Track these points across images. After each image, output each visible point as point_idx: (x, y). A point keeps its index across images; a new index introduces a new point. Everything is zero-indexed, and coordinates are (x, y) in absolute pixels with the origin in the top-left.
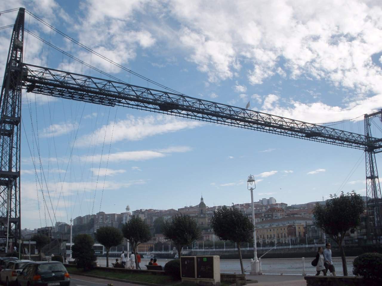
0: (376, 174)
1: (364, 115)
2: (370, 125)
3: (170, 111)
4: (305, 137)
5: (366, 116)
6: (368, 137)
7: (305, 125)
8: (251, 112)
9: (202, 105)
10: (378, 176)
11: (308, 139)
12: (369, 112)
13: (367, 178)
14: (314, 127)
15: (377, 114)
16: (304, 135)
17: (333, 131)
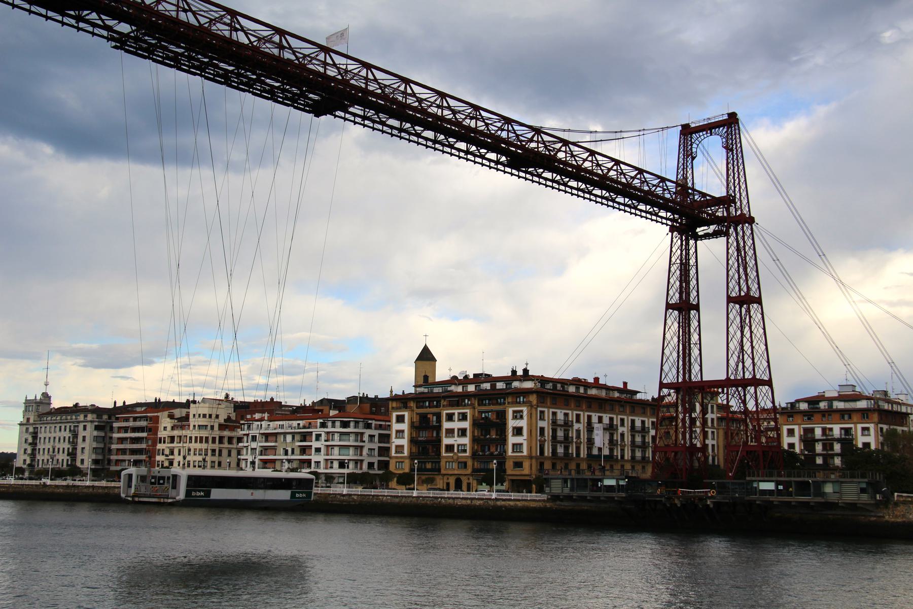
0: (693, 300)
1: (680, 128)
2: (693, 158)
3: (72, 13)
4: (504, 166)
5: (687, 131)
6: (683, 187)
7: (510, 128)
8: (350, 62)
9: (189, 14)
10: (698, 304)
11: (514, 171)
12: (696, 118)
13: (669, 306)
14: (535, 139)
15: (715, 128)
16: (503, 159)
17: (590, 158)
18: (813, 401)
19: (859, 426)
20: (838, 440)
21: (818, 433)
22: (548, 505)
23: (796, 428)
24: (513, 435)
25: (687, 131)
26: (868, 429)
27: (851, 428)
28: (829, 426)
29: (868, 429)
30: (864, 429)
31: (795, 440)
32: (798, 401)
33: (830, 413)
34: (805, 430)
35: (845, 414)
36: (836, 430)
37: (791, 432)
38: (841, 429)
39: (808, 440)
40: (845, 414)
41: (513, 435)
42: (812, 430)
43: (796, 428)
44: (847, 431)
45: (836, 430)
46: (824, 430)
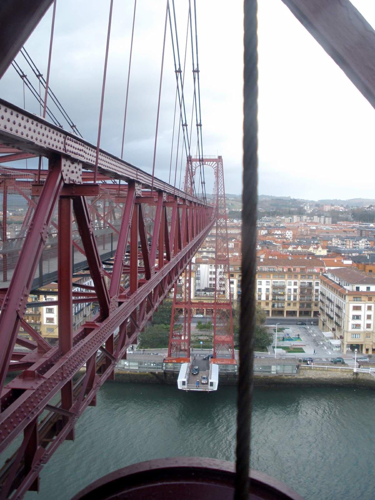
24: (47, 312)
41: (47, 312)
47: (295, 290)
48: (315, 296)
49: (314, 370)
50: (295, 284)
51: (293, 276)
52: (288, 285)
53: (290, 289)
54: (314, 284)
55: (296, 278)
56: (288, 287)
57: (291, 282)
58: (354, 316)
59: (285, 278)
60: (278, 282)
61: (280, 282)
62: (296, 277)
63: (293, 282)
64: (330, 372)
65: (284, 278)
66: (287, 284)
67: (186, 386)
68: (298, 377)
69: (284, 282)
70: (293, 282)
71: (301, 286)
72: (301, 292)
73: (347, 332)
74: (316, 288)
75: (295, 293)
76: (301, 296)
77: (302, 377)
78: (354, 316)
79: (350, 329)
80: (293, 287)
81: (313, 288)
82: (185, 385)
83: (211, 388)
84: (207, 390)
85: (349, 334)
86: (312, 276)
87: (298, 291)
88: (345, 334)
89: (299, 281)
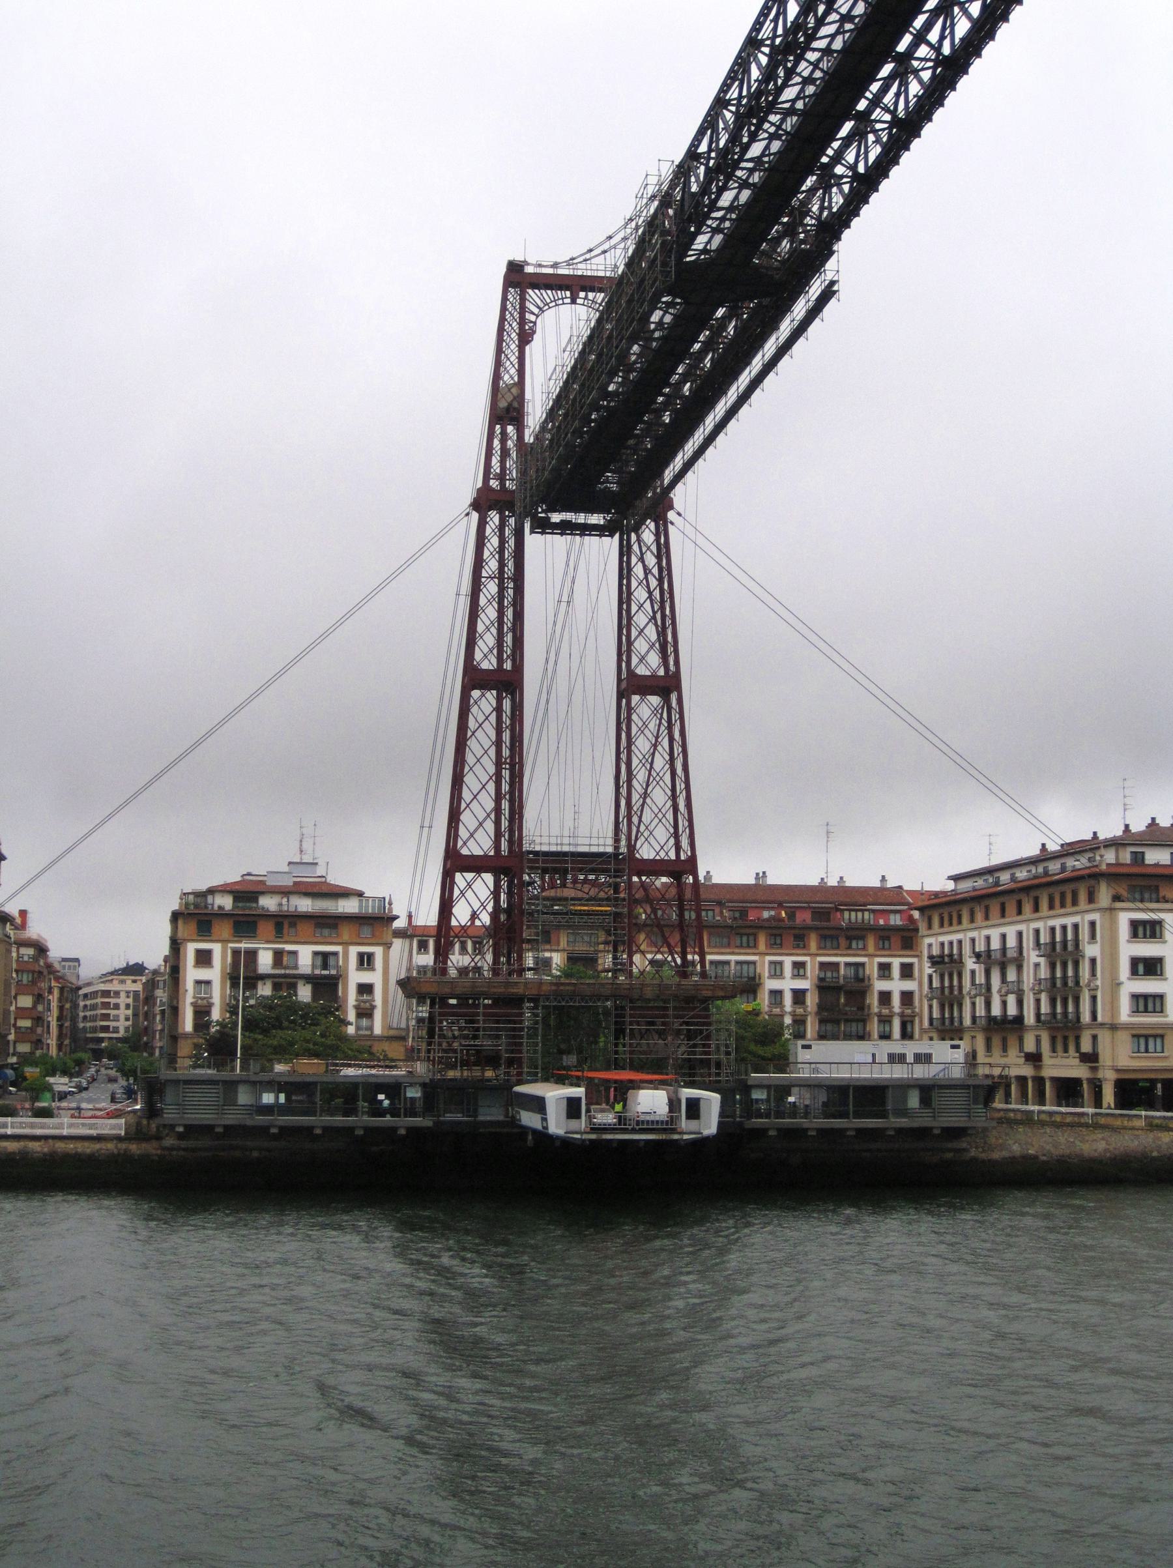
5: (517, 277)
18: (246, 893)
19: (354, 951)
20: (308, 979)
21: (265, 961)
22: (134, 1148)
23: (216, 948)
25: (517, 277)
26: (370, 956)
27: (336, 954)
28: (289, 947)
29: (370, 956)
30: (361, 956)
31: (214, 974)
32: (212, 891)
33: (284, 924)
34: (236, 953)
35: (327, 924)
36: (305, 956)
37: (204, 959)
38: (316, 954)
39: (243, 974)
40: (327, 924)
42: (252, 955)
43: (216, 948)
44: (325, 956)
45: (305, 956)
46: (278, 955)
47: (799, 996)
48: (880, 1021)
49: (1043, 1124)
50: (799, 966)
51: (789, 940)
52: (771, 977)
53: (777, 994)
54: (872, 970)
55: (798, 947)
56: (771, 984)
57: (781, 963)
58: (1135, 962)
59: (755, 946)
60: (728, 963)
61: (737, 963)
62: (800, 940)
63: (788, 961)
64: (1107, 1134)
65: (752, 946)
66: (767, 974)
67: (582, 1124)
68: (983, 1156)
69: (754, 963)
70: (788, 961)
71: (821, 980)
72: (821, 1007)
73: (1114, 1027)
74: (880, 985)
75: (800, 1011)
76: (821, 1022)
77: (996, 1155)
78: (1135, 962)
79: (1125, 1013)
80: (788, 984)
81: (869, 987)
82: (578, 1117)
83: (692, 1125)
84: (676, 1137)
85: (1124, 1038)
86: (863, 938)
87: (811, 1000)
88: (1104, 1037)
89: (812, 965)
